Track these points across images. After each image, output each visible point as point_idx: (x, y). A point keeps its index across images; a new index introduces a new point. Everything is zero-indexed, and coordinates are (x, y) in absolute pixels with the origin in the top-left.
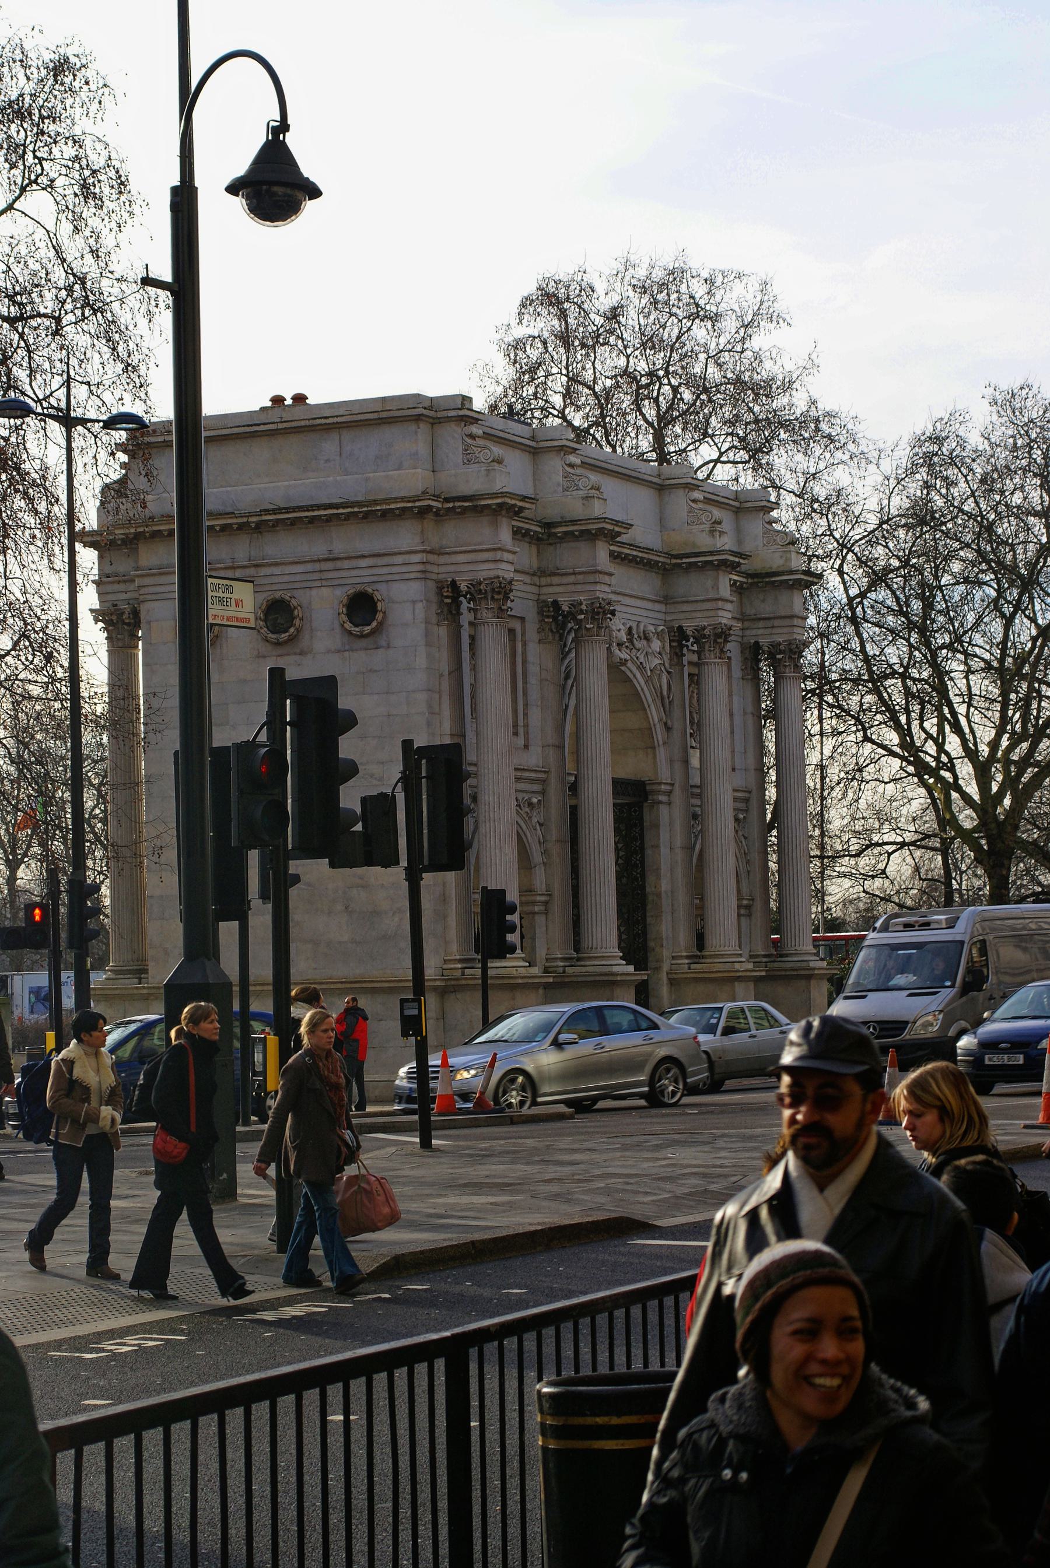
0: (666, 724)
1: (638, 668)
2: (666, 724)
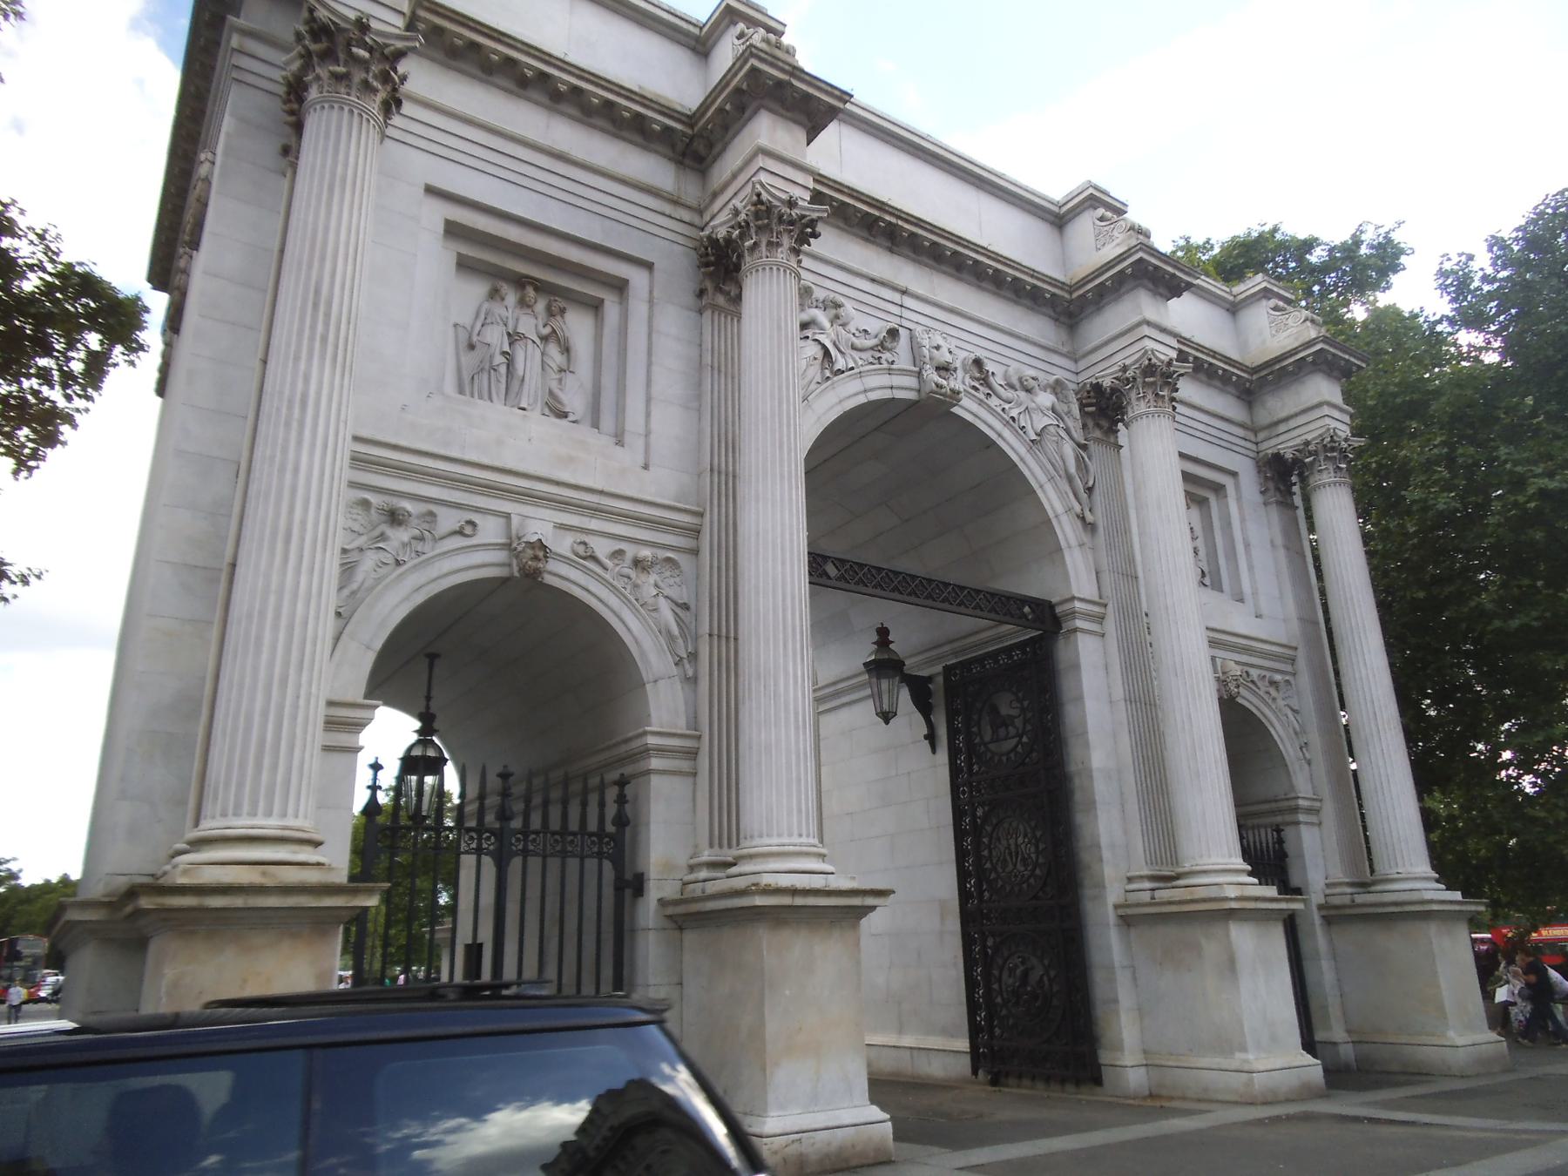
0: (1083, 519)
2: (1083, 519)
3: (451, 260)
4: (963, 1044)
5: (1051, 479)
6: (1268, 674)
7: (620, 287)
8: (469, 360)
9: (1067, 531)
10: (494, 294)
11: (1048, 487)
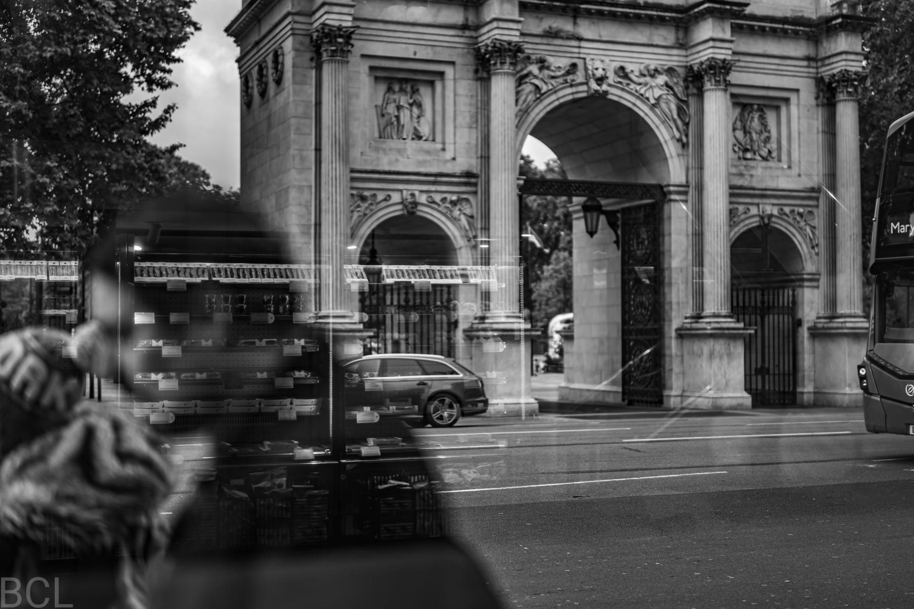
1: (638, 97)
3: (372, 79)
4: (620, 389)
5: (663, 122)
6: (796, 209)
7: (441, 74)
8: (383, 121)
9: (671, 149)
10: (390, 90)
11: (662, 128)
